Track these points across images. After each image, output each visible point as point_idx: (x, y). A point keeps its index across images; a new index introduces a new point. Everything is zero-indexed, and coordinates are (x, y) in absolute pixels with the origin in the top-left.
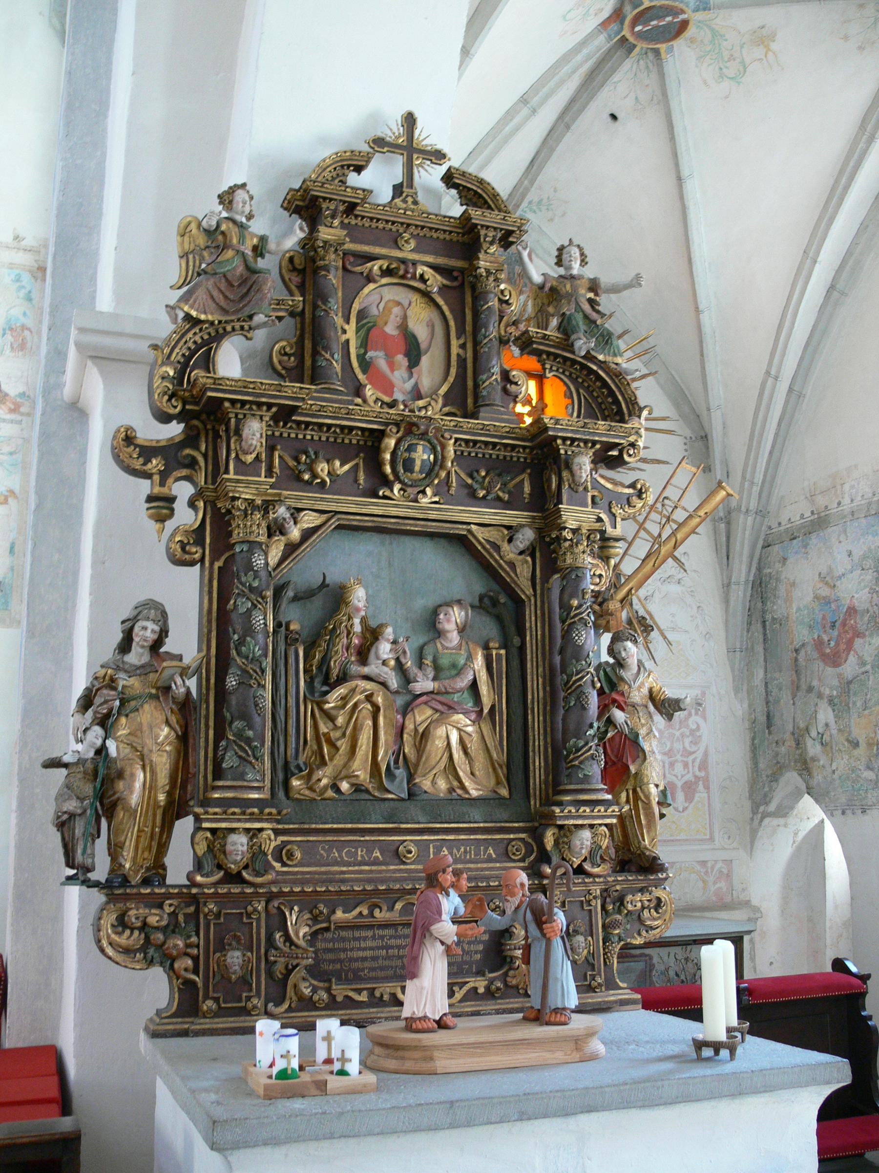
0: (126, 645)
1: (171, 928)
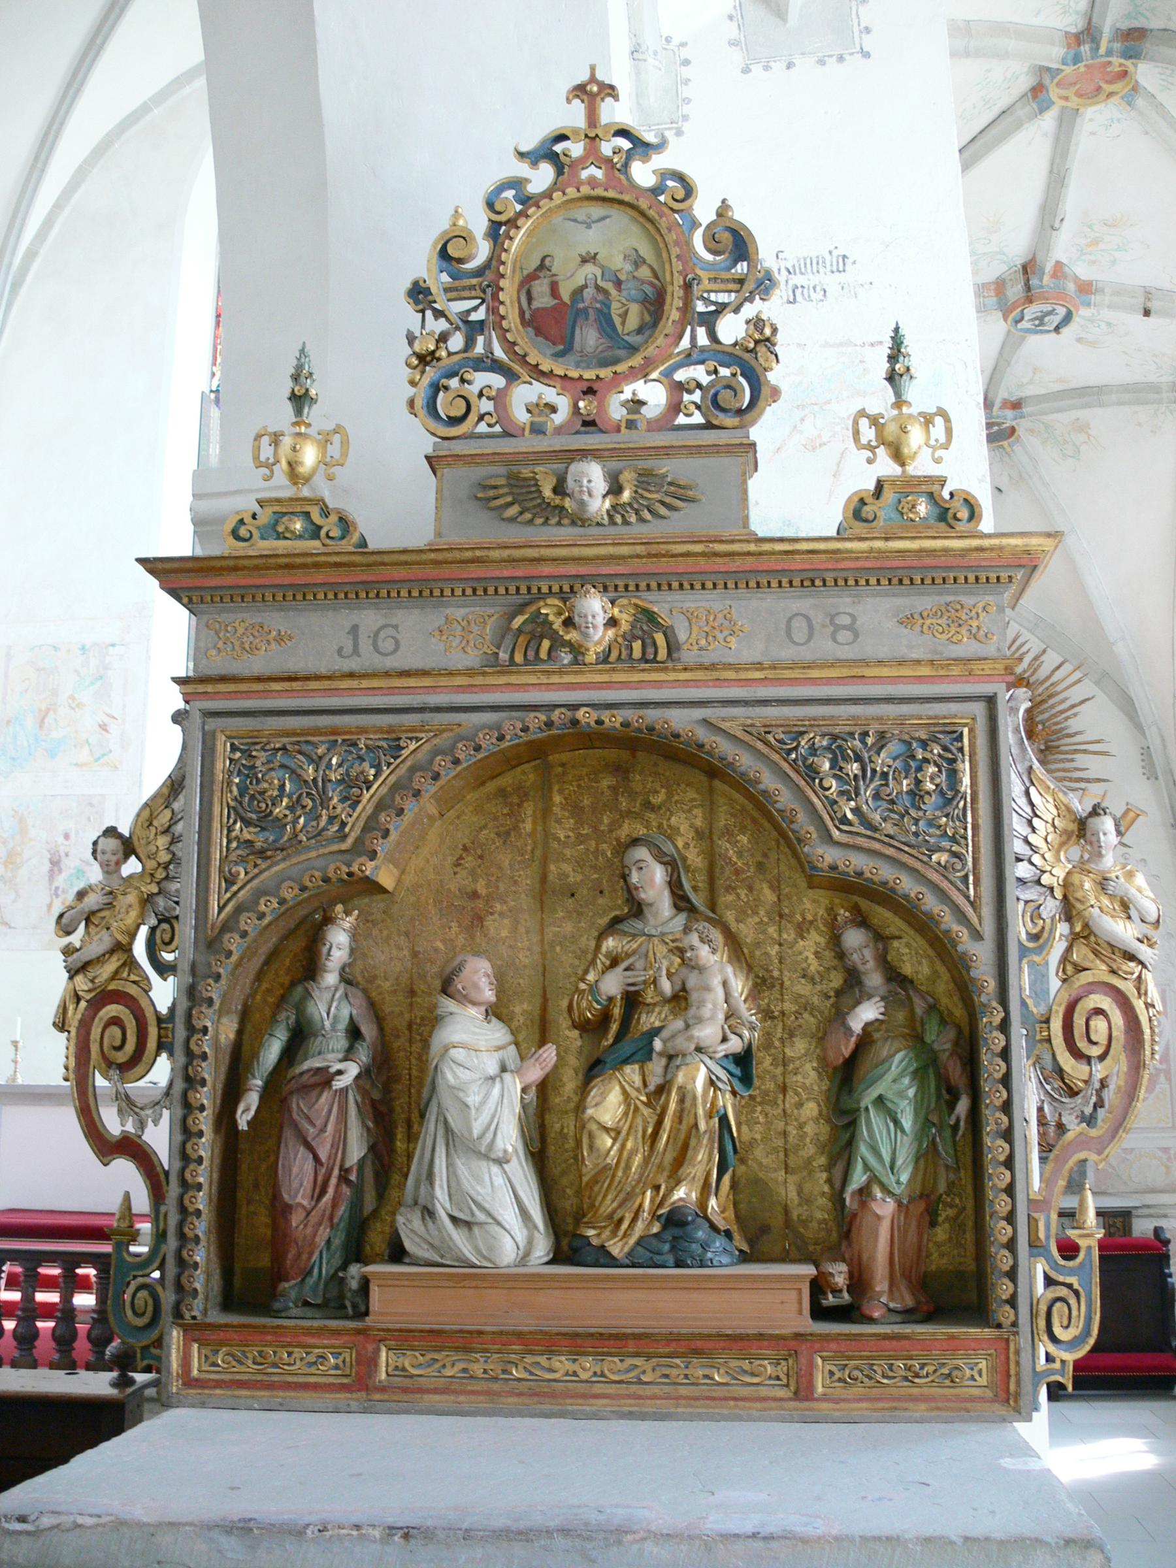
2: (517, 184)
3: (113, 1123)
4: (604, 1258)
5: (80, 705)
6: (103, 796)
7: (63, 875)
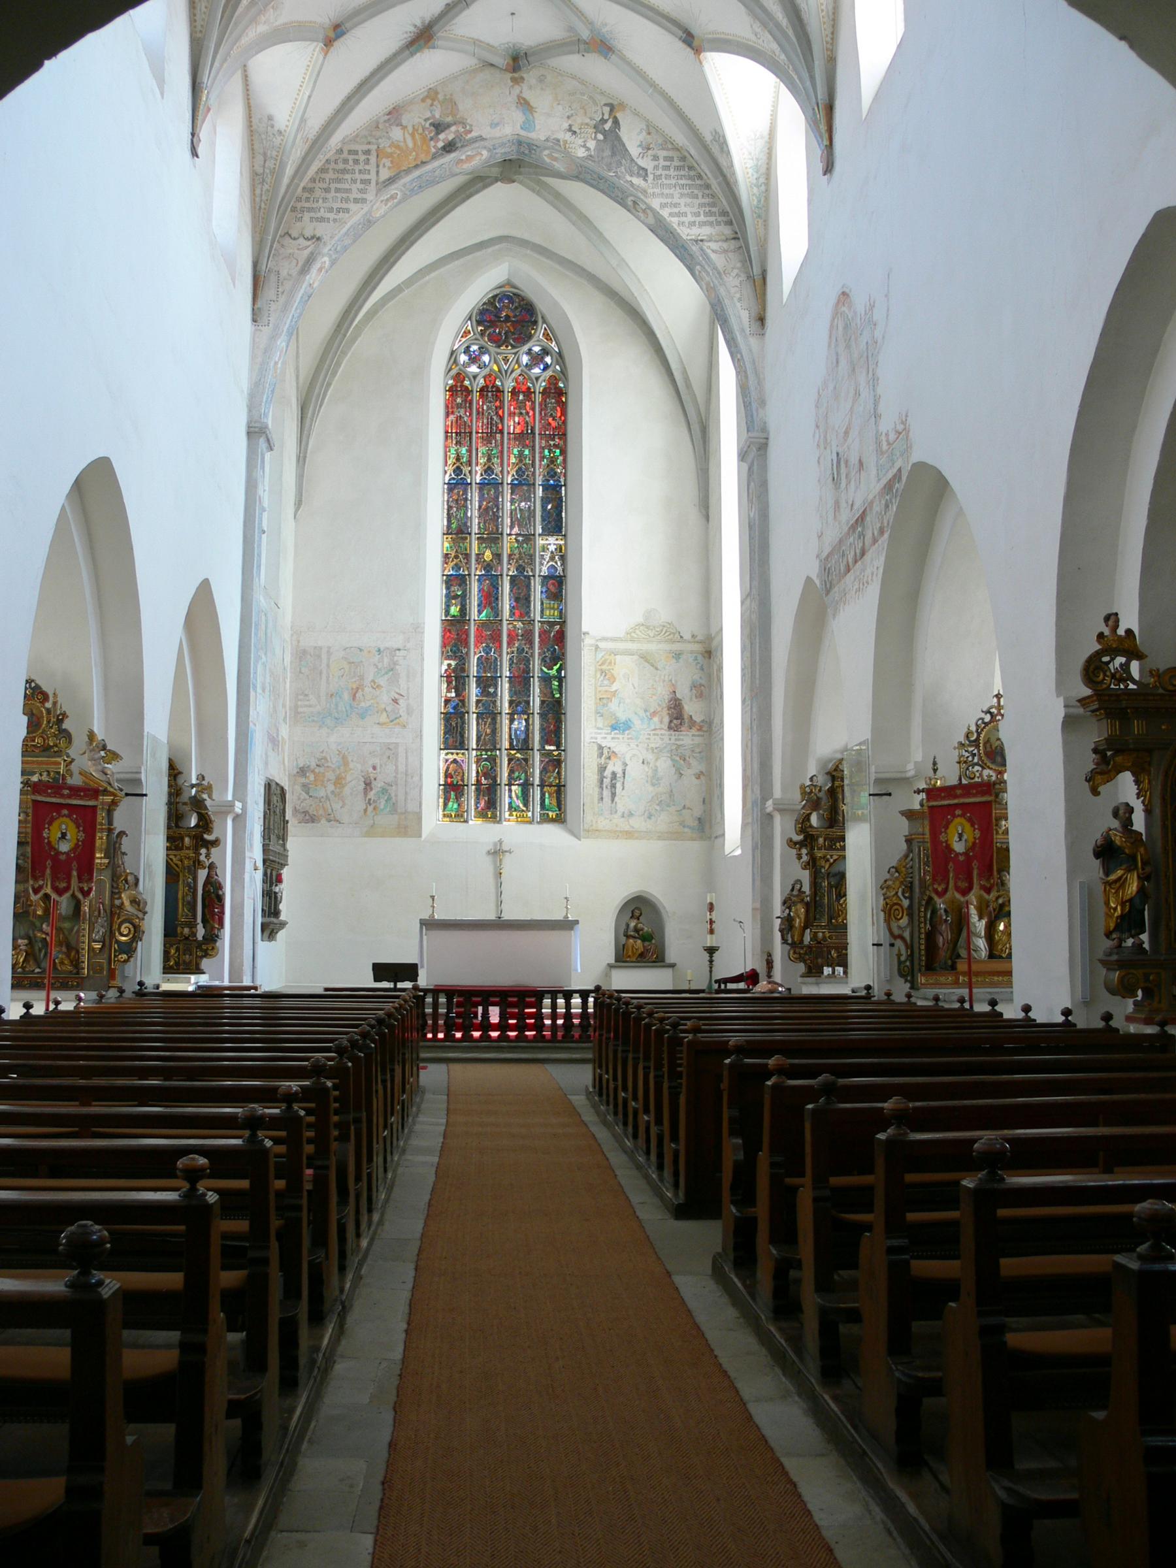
0: (792, 890)
1: (806, 953)
2: (982, 719)
4: (1002, 958)
5: (379, 686)
6: (397, 744)
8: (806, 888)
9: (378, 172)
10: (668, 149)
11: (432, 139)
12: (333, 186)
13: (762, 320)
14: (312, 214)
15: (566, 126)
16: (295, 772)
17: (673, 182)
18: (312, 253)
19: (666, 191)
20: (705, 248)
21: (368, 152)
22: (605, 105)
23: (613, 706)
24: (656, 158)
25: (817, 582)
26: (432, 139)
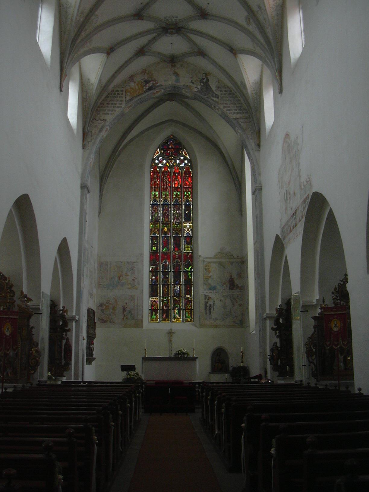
0: (273, 346)
2: (340, 283)
3: (311, 361)
5: (128, 275)
6: (134, 295)
7: (126, 312)
8: (279, 345)
9: (126, 98)
10: (226, 88)
11: (144, 86)
12: (110, 102)
13: (259, 145)
14: (103, 112)
15: (190, 81)
16: (99, 305)
17: (228, 99)
18: (103, 125)
19: (225, 102)
20: (239, 121)
21: (122, 91)
22: (204, 74)
23: (210, 281)
24: (221, 91)
25: (280, 236)
26: (144, 86)
